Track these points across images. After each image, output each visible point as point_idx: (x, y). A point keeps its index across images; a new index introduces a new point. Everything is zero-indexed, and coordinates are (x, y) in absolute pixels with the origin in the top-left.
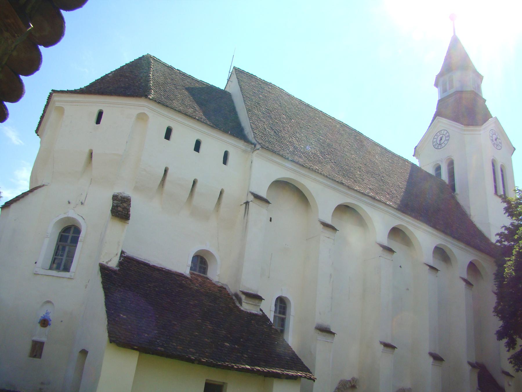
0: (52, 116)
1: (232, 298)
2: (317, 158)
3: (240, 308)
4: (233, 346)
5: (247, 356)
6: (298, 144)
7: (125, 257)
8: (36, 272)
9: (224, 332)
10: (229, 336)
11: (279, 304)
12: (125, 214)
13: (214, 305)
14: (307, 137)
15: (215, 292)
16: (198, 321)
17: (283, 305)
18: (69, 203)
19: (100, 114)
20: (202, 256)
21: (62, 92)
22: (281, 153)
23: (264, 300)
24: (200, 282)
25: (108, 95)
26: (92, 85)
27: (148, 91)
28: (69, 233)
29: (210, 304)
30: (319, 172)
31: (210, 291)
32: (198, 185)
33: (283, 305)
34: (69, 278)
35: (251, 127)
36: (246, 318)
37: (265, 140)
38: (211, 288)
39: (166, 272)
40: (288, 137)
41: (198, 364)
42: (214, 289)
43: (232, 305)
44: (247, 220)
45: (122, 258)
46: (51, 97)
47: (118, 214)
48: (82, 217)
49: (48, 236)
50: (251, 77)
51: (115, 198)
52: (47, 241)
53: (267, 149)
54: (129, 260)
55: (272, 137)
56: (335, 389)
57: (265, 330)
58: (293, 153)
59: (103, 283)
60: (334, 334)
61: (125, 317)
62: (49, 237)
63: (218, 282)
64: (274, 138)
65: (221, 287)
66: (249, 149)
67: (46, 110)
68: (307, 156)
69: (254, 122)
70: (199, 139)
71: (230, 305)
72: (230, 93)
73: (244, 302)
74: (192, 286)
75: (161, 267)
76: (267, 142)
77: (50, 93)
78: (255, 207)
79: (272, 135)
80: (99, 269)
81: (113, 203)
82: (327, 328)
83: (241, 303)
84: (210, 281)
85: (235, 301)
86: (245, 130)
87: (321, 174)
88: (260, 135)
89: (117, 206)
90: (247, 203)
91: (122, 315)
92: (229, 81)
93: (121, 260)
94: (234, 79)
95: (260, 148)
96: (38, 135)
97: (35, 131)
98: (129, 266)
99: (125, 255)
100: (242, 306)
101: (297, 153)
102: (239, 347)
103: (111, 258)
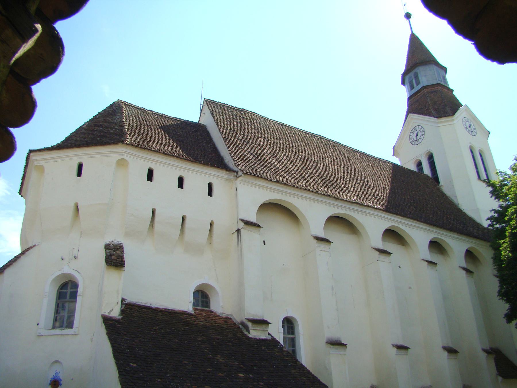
0: (33, 175)
2: (299, 174)
3: (249, 336)
4: (248, 376)
5: (263, 384)
6: (279, 164)
7: (126, 304)
8: (40, 333)
9: (236, 363)
10: (242, 366)
11: (286, 325)
12: (119, 261)
13: (222, 337)
14: (287, 156)
15: (220, 324)
16: (209, 356)
17: (290, 325)
18: (63, 259)
19: (80, 166)
20: (202, 290)
21: (40, 150)
22: (264, 176)
23: (271, 323)
24: (204, 317)
25: (85, 146)
26: (68, 139)
27: (124, 136)
28: (67, 289)
29: (218, 337)
30: (304, 188)
31: (216, 323)
32: (187, 221)
35: (230, 155)
36: (256, 345)
37: (246, 166)
38: (217, 321)
39: (170, 312)
40: (268, 159)
42: (220, 321)
43: (240, 334)
44: (241, 247)
45: (123, 306)
46: (29, 157)
47: (112, 263)
48: (77, 271)
49: (46, 295)
50: (223, 106)
51: (107, 247)
52: (45, 301)
54: (130, 307)
55: (252, 162)
57: (277, 353)
58: (275, 174)
59: (108, 334)
60: (345, 345)
61: (135, 365)
62: (47, 296)
63: (223, 313)
64: (254, 162)
65: (227, 318)
66: (232, 177)
67: (27, 170)
68: (289, 174)
69: (232, 150)
70: (180, 176)
71: (238, 335)
72: (205, 124)
73: (252, 329)
74: (197, 322)
75: (164, 307)
76: (248, 168)
77: (28, 153)
78: (247, 233)
79: (252, 160)
80: (102, 321)
81: (106, 252)
82: (338, 341)
83: (248, 331)
84: (215, 315)
85: (242, 329)
86: (225, 159)
87: (306, 190)
88: (241, 161)
89: (111, 255)
90: (238, 231)
91: (132, 364)
92: (202, 114)
93: (123, 308)
94: (206, 110)
95: (243, 175)
96: (22, 196)
97: (19, 192)
98: (131, 312)
99: (125, 302)
100: (250, 333)
101: (279, 173)
102: (253, 376)
103: (113, 308)
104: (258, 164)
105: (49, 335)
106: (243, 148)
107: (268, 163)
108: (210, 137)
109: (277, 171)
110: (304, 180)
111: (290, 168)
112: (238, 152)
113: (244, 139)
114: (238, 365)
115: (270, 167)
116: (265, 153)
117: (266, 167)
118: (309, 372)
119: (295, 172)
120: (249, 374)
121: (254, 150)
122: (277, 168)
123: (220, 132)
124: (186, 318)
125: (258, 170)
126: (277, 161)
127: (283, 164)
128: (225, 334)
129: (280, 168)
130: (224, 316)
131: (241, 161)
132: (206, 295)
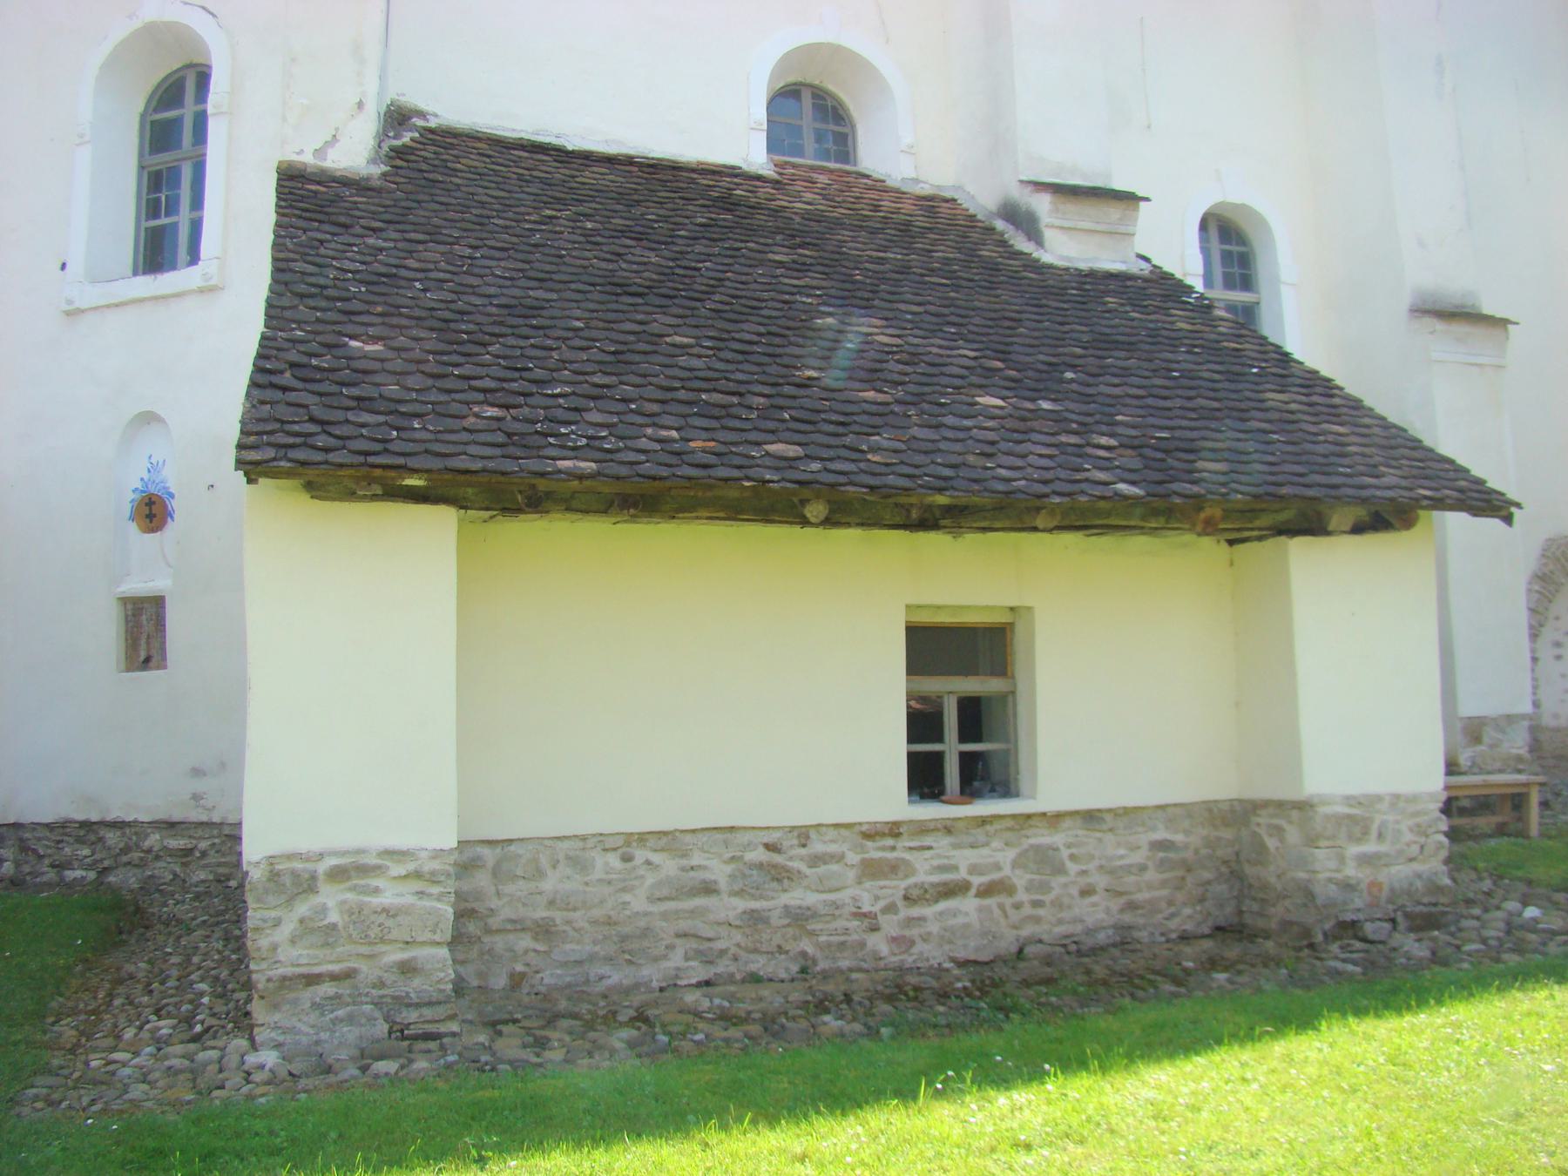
1: (992, 230)
3: (1037, 261)
5: (1113, 442)
8: (70, 302)
11: (1216, 247)
17: (1235, 248)
20: (817, 82)
33: (1235, 248)
34: (201, 291)
41: (829, 522)
48: (204, 8)
49: (81, 136)
56: (1530, 583)
60: (1503, 323)
63: (916, 181)
73: (1052, 227)
82: (1463, 307)
83: (1035, 236)
84: (879, 186)
99: (428, 121)
103: (337, 129)
105: (108, 306)
120: (1033, 400)
124: (732, 186)
130: (925, 190)
132: (834, 108)
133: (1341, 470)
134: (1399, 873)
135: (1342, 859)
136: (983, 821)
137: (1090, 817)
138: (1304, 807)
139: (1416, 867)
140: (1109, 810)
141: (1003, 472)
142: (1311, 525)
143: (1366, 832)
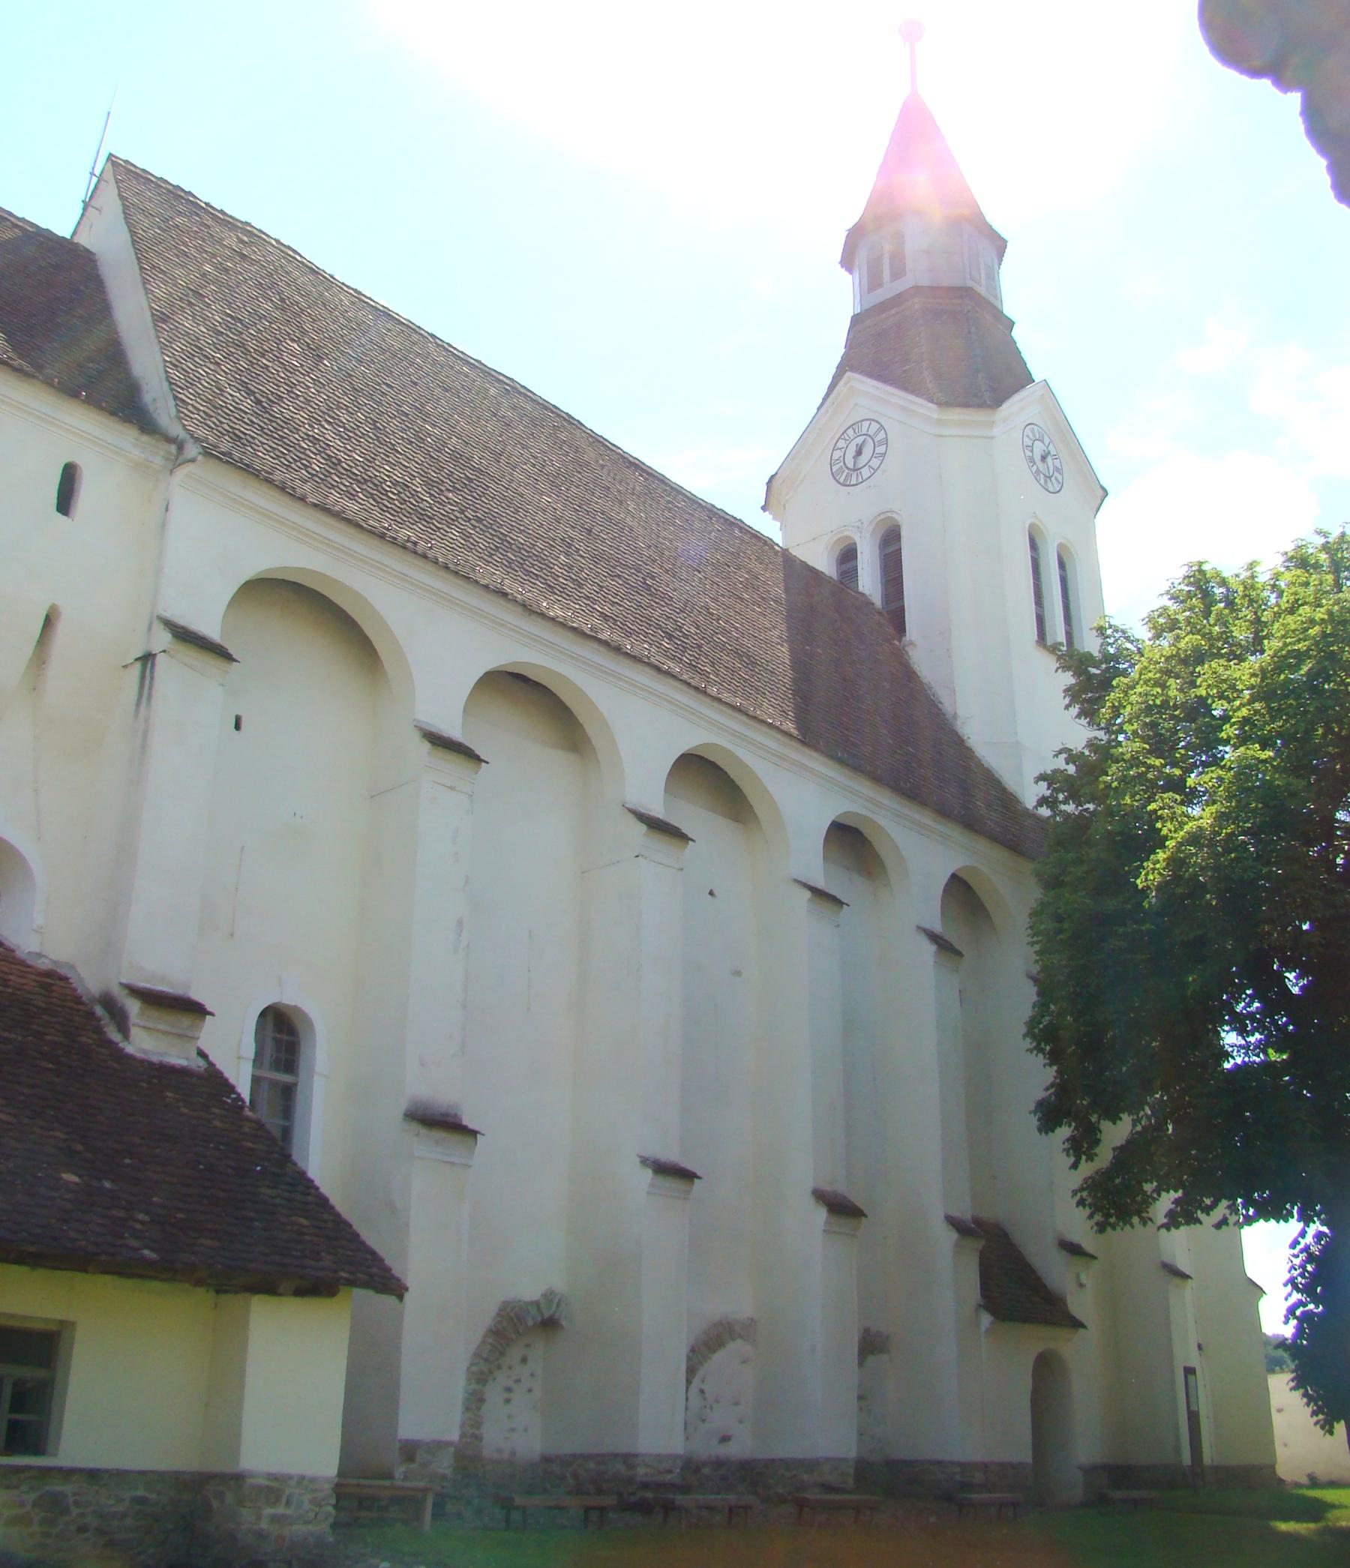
1: (91, 1014)
2: (411, 500)
3: (122, 1050)
4: (96, 1183)
5: (146, 1218)
6: (342, 449)
10: (80, 1147)
11: (270, 1032)
14: (378, 425)
17: (285, 1038)
22: (277, 477)
30: (419, 550)
31: (8, 987)
33: (285, 1038)
35: (168, 378)
37: (220, 429)
40: (306, 421)
42: (23, 981)
44: (147, 721)
50: (177, 196)
53: (226, 460)
55: (246, 420)
57: (217, 1123)
58: (322, 480)
63: (39, 955)
64: (251, 421)
65: (50, 974)
66: (158, 460)
68: (375, 492)
69: (177, 360)
72: (94, 251)
73: (139, 1026)
76: (227, 438)
79: (246, 413)
83: (124, 1030)
85: (102, 1022)
86: (145, 388)
87: (425, 556)
88: (202, 408)
90: (147, 659)
92: (90, 208)
94: (110, 197)
95: (200, 457)
101: (337, 479)
104: (266, 431)
106: (218, 364)
107: (302, 435)
108: (106, 300)
109: (332, 471)
110: (425, 524)
111: (379, 472)
112: (197, 375)
113: (228, 333)
114: (64, 1140)
115: (308, 452)
116: (301, 399)
117: (291, 449)
118: (323, 1202)
119: (398, 488)
121: (261, 378)
122: (334, 460)
123: (146, 288)
125: (260, 454)
126: (340, 436)
127: (358, 452)
128: (35, 1027)
129: (344, 465)
130: (43, 964)
131: (202, 408)
133: (294, 1253)
134: (299, 1529)
135: (259, 1518)
136: (18, 1470)
137: (93, 1475)
138: (239, 1478)
139: (311, 1528)
140: (107, 1471)
141: (73, 1234)
142: (268, 1287)
143: (278, 1499)
